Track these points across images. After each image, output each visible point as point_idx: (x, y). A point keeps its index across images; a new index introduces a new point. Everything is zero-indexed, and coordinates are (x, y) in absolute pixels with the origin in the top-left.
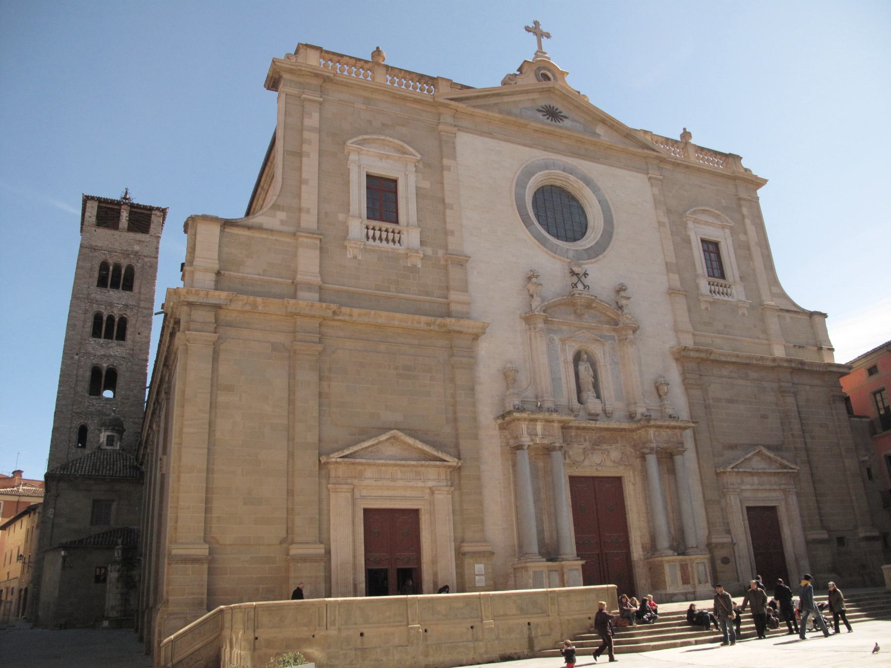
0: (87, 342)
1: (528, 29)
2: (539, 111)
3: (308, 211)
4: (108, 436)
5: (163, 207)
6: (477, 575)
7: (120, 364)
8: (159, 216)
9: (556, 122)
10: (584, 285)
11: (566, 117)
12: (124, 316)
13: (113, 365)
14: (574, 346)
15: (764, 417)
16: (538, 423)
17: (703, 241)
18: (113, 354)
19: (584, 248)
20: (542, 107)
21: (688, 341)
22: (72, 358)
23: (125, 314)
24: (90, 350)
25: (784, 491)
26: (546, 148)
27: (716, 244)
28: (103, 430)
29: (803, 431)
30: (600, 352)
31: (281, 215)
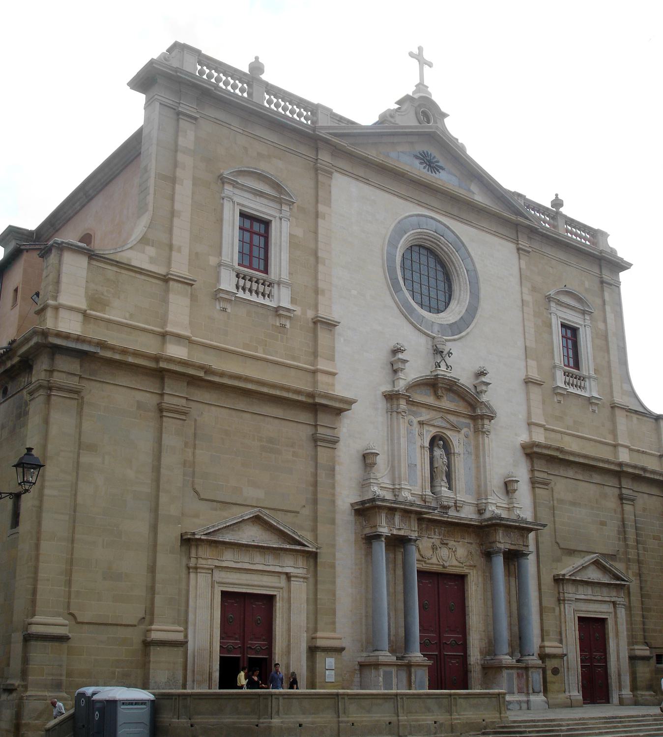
1: (411, 55)
2: (416, 157)
3: (179, 250)
6: (327, 669)
9: (432, 173)
10: (447, 365)
11: (443, 169)
14: (431, 431)
15: (603, 524)
16: (396, 513)
17: (563, 326)
19: (449, 323)
20: (419, 153)
21: (539, 437)
25: (614, 603)
26: (420, 204)
27: (574, 331)
29: (638, 542)
30: (457, 440)
31: (151, 251)
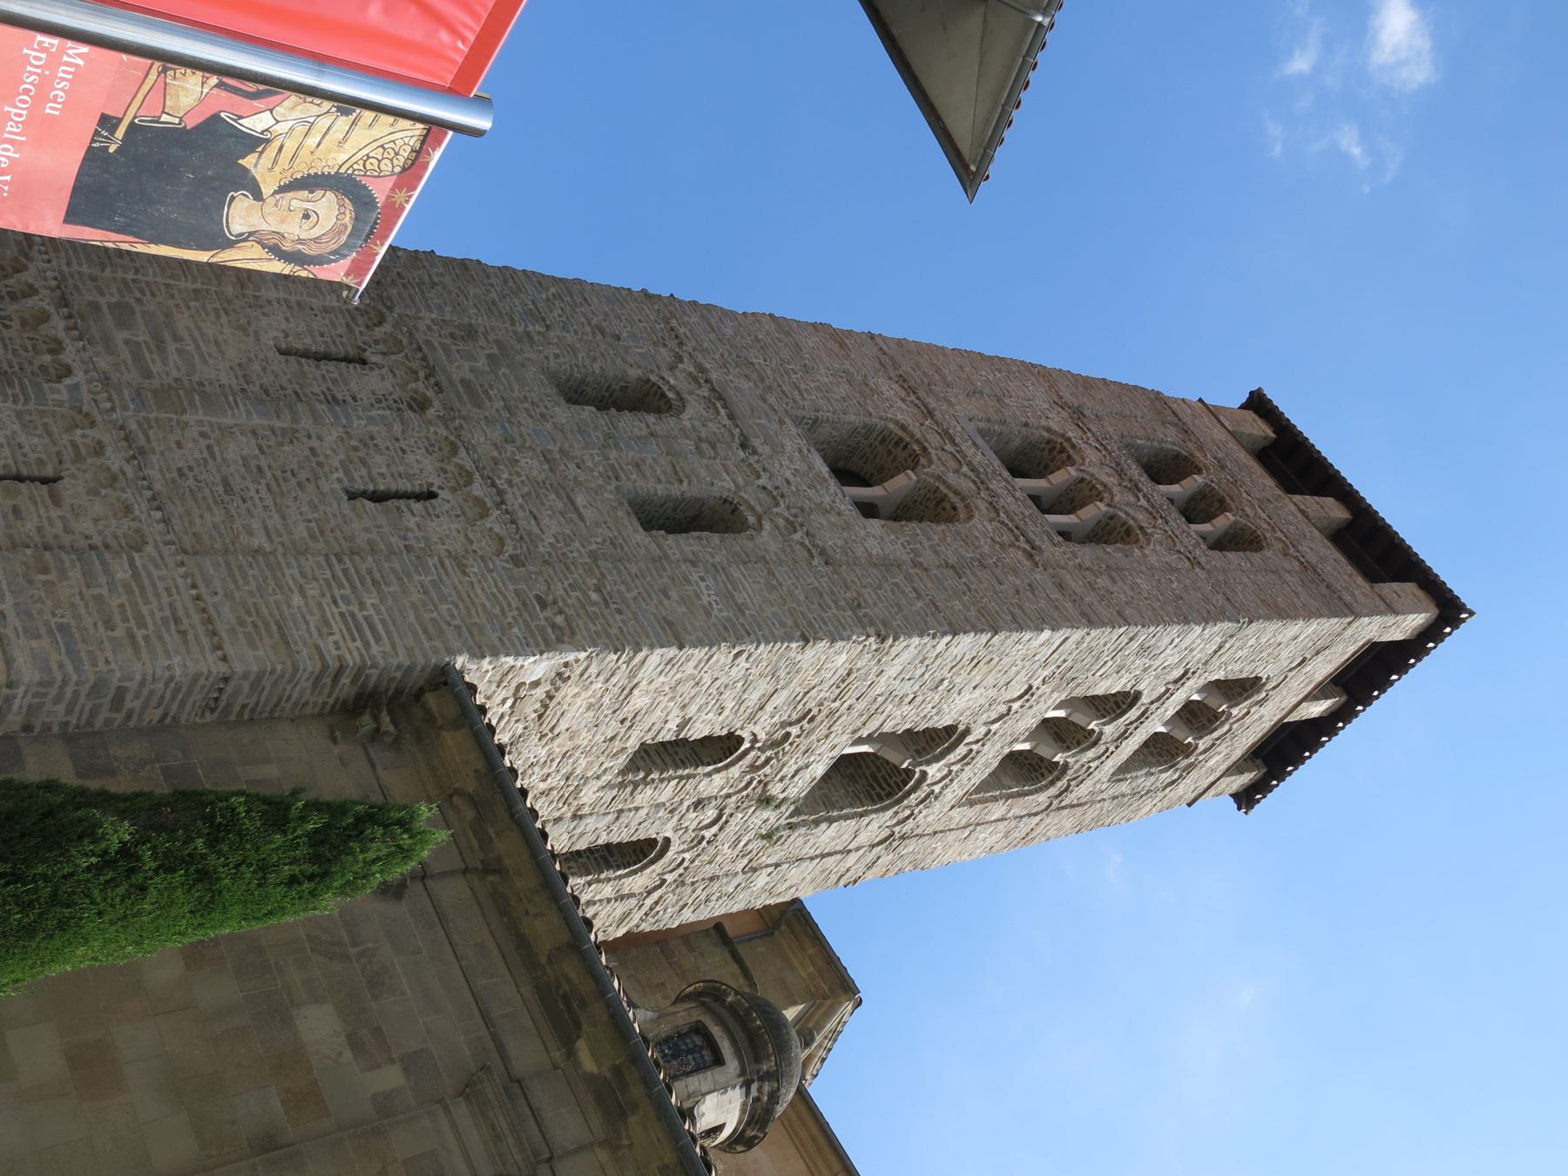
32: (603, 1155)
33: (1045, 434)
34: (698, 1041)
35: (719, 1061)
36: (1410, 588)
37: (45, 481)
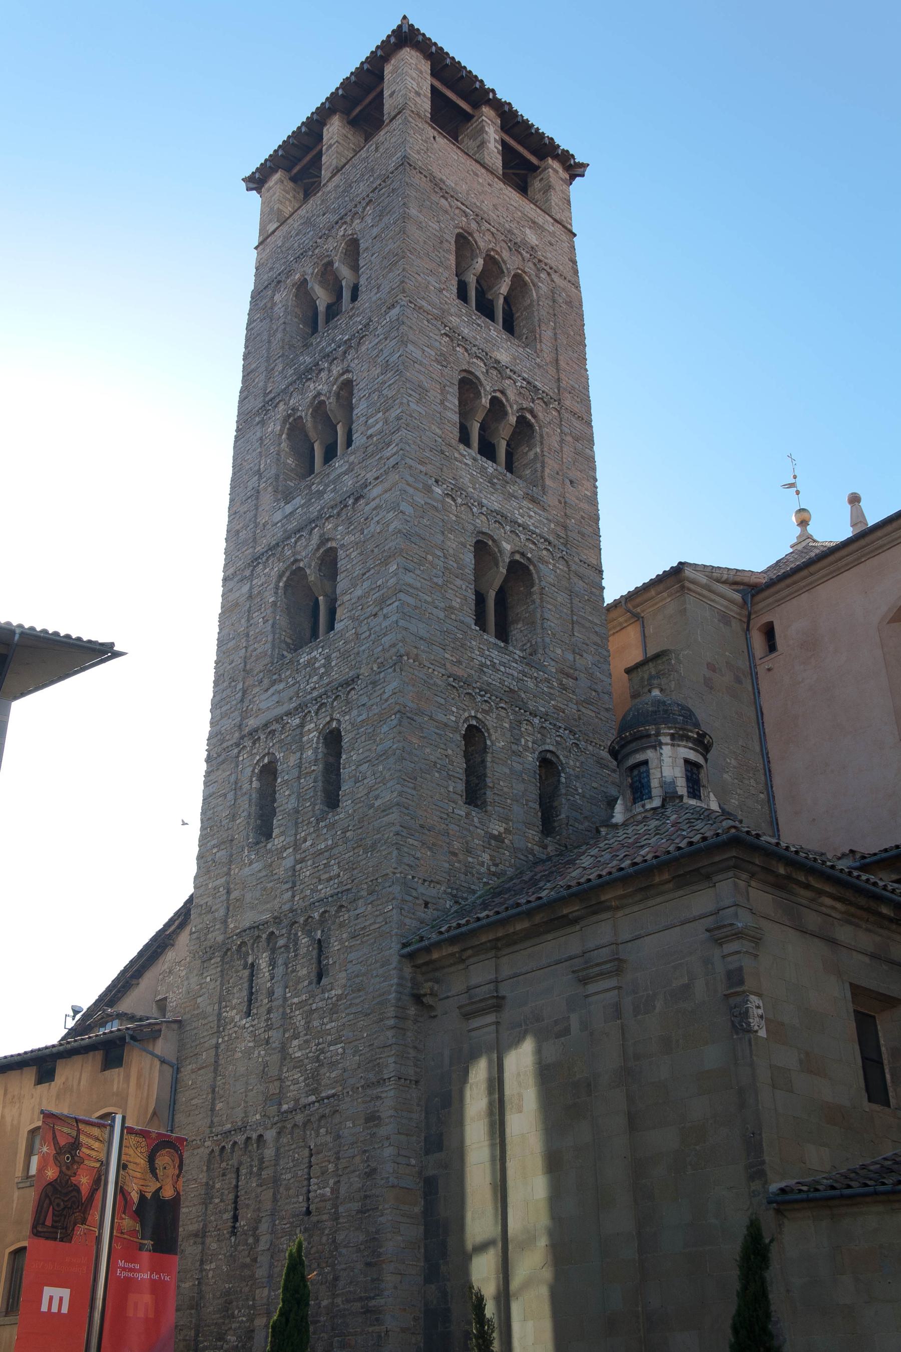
0: (456, 455)
4: (687, 761)
5: (578, 159)
7: (541, 559)
8: (562, 179)
12: (529, 416)
13: (523, 555)
18: (519, 521)
22: (428, 490)
23: (531, 412)
24: (466, 480)
28: (666, 739)
32: (620, 914)
33: (284, 436)
34: (636, 772)
35: (646, 763)
36: (388, 69)
37: (311, 1155)
